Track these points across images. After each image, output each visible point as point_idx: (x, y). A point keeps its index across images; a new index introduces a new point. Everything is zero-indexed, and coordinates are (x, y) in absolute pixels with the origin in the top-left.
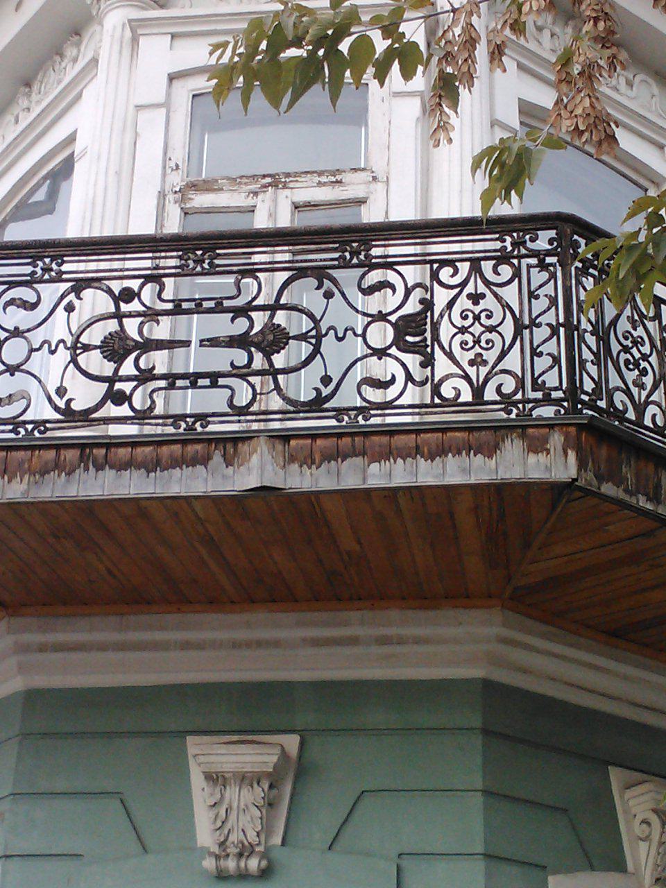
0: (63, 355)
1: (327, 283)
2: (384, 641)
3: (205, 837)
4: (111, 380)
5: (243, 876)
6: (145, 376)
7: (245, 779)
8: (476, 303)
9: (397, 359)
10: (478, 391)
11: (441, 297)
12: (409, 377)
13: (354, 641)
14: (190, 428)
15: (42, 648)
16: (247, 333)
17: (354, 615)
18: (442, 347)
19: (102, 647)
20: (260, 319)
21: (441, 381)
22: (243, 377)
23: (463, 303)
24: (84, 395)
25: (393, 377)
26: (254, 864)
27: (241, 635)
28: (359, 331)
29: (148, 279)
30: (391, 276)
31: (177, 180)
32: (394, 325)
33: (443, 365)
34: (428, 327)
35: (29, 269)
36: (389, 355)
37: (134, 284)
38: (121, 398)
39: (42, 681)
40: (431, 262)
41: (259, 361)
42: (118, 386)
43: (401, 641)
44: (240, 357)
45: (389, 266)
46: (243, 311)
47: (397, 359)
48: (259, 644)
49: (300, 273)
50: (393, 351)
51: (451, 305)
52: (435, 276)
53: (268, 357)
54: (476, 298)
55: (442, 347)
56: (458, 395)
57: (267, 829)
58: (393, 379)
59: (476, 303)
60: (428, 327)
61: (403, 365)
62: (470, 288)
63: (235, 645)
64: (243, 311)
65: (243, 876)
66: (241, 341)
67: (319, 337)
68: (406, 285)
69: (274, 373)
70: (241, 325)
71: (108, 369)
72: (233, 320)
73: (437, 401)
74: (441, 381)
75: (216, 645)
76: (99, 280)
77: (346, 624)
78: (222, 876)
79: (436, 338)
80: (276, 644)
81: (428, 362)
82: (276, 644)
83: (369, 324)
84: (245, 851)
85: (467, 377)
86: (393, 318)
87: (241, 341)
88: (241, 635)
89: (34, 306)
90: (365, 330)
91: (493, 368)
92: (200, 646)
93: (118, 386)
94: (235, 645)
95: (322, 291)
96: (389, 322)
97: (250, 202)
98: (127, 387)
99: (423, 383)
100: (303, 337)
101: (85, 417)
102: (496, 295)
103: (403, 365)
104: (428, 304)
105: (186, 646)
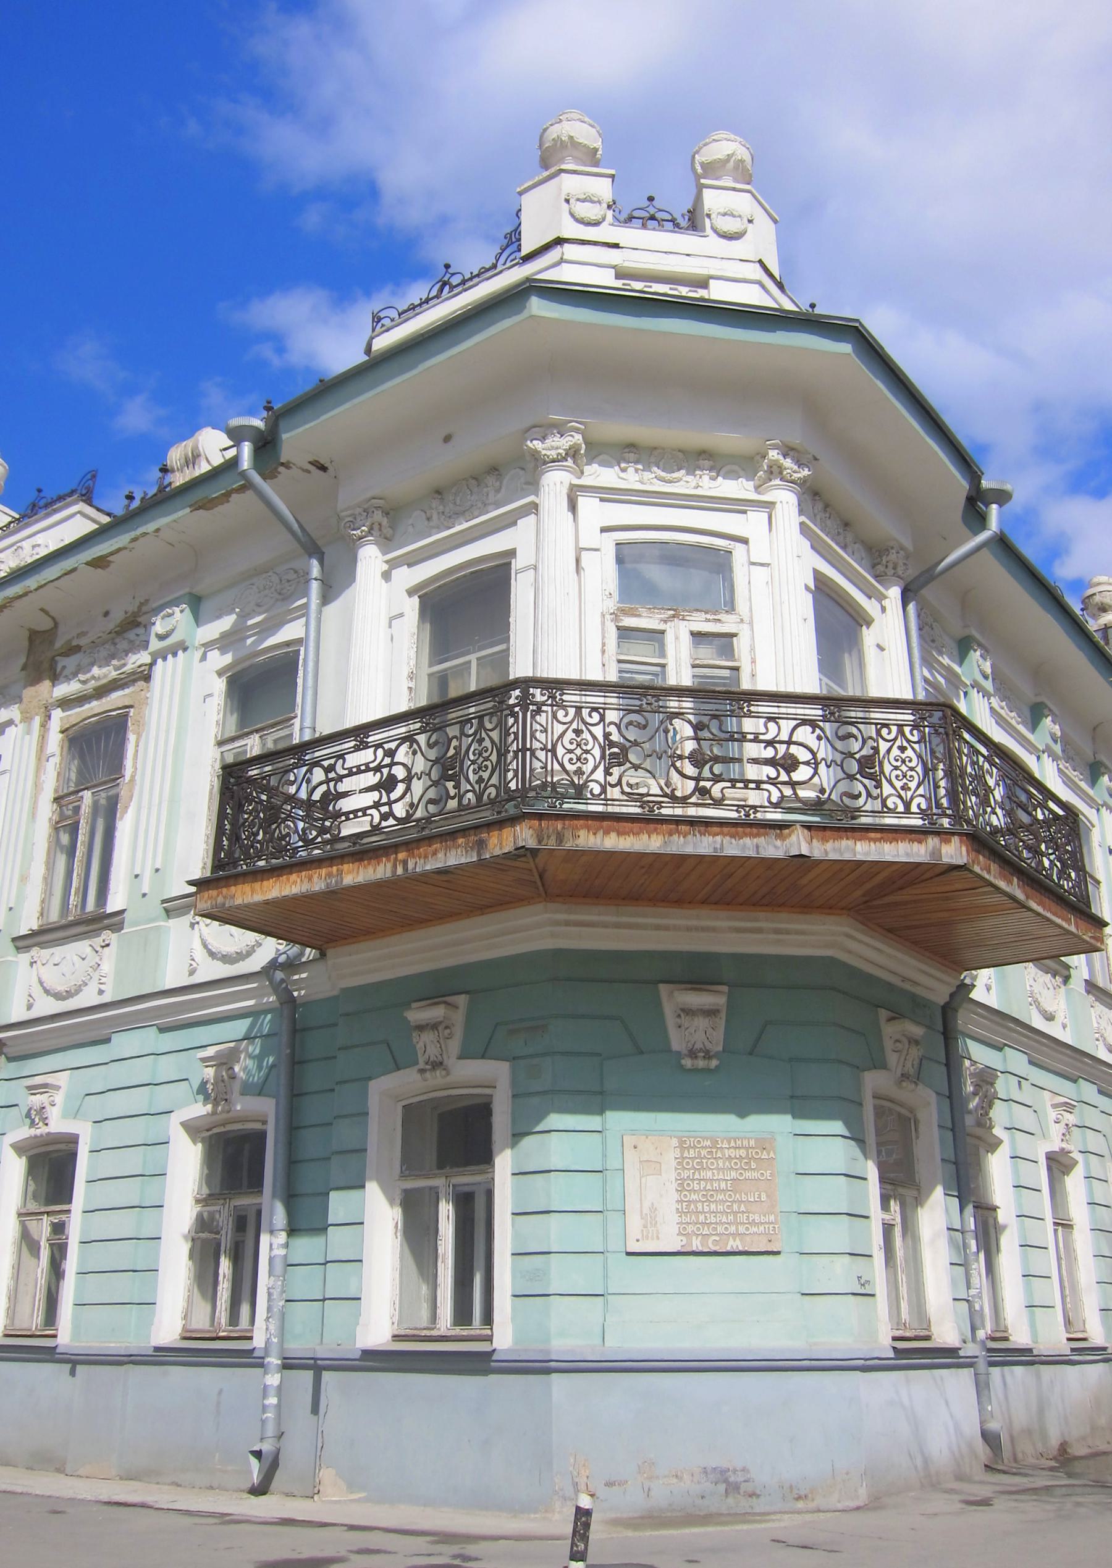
1: (818, 731)
2: (777, 931)
3: (677, 1043)
4: (697, 779)
5: (707, 1071)
6: (717, 779)
8: (903, 752)
9: (861, 782)
10: (907, 805)
11: (883, 746)
12: (869, 795)
13: (760, 931)
14: (747, 815)
15: (567, 923)
16: (774, 757)
17: (762, 915)
18: (886, 778)
19: (605, 925)
20: (782, 749)
21: (887, 797)
22: (774, 784)
23: (895, 752)
25: (860, 792)
26: (714, 1063)
27: (694, 923)
28: (839, 763)
29: (714, 717)
30: (854, 731)
31: (612, 605)
32: (858, 761)
33: (887, 789)
34: (877, 763)
35: (638, 703)
36: (857, 779)
37: (705, 719)
40: (876, 724)
41: (784, 777)
42: (702, 783)
43: (788, 932)
44: (772, 772)
45: (852, 724)
46: (770, 743)
47: (861, 782)
48: (704, 929)
49: (804, 722)
50: (858, 776)
51: (889, 751)
52: (878, 732)
53: (788, 773)
54: (902, 749)
55: (886, 778)
56: (896, 808)
58: (860, 795)
59: (903, 752)
60: (877, 763)
61: (865, 786)
62: (898, 743)
63: (689, 929)
64: (770, 743)
66: (771, 762)
67: (817, 764)
68: (863, 737)
70: (769, 753)
72: (765, 748)
73: (885, 810)
74: (887, 797)
75: (676, 928)
76: (683, 714)
77: (756, 920)
79: (882, 772)
80: (714, 930)
81: (879, 786)
82: (714, 930)
83: (845, 758)
85: (900, 797)
86: (857, 756)
87: (771, 762)
88: (694, 923)
89: (645, 727)
90: (842, 763)
91: (914, 792)
92: (666, 928)
93: (702, 783)
94: (689, 929)
95: (815, 734)
96: (855, 758)
97: (662, 627)
98: (708, 784)
99: (876, 798)
100: (807, 763)
101: (684, 801)
102: (913, 749)
103: (865, 786)
104: (876, 750)
105: (658, 928)
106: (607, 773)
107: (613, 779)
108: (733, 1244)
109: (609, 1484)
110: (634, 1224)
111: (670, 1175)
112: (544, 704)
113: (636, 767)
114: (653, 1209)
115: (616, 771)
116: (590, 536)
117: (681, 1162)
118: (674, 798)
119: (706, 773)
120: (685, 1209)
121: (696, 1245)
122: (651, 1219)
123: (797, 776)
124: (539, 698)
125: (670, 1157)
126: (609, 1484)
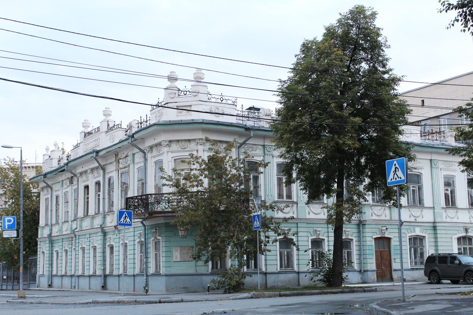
0: (165, 203)
3: (180, 235)
4: (169, 205)
5: (183, 238)
7: (183, 230)
15: (166, 219)
24: (167, 207)
38: (169, 207)
39: (166, 222)
57: (185, 234)
65: (183, 238)
69: (180, 205)
71: (168, 204)
78: (182, 238)
84: (183, 236)
98: (170, 206)
106: (158, 206)
107: (158, 206)
108: (187, 260)
109: (172, 289)
110: (174, 258)
111: (179, 252)
112: (140, 205)
113: (161, 204)
114: (177, 256)
115: (159, 205)
116: (170, 159)
117: (180, 250)
118: (166, 208)
119: (170, 204)
120: (181, 256)
121: (182, 260)
122: (176, 257)
123: (181, 204)
124: (149, 197)
125: (179, 249)
126: (172, 289)
